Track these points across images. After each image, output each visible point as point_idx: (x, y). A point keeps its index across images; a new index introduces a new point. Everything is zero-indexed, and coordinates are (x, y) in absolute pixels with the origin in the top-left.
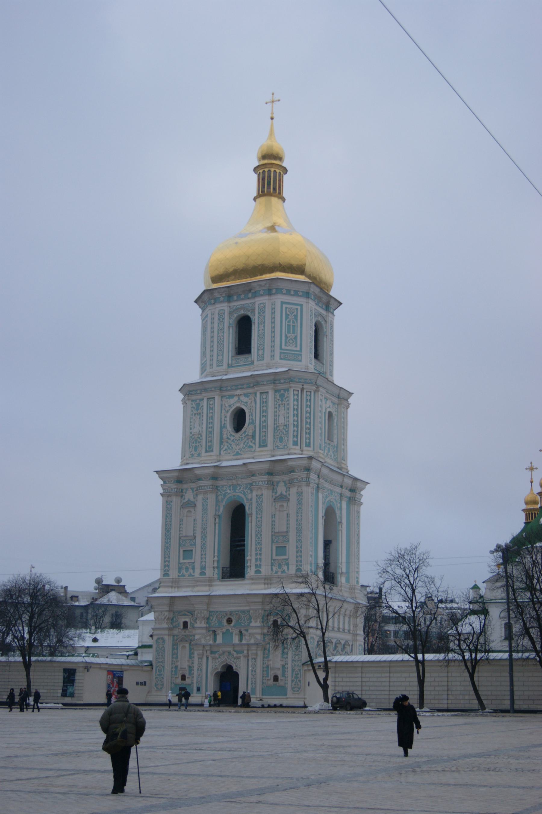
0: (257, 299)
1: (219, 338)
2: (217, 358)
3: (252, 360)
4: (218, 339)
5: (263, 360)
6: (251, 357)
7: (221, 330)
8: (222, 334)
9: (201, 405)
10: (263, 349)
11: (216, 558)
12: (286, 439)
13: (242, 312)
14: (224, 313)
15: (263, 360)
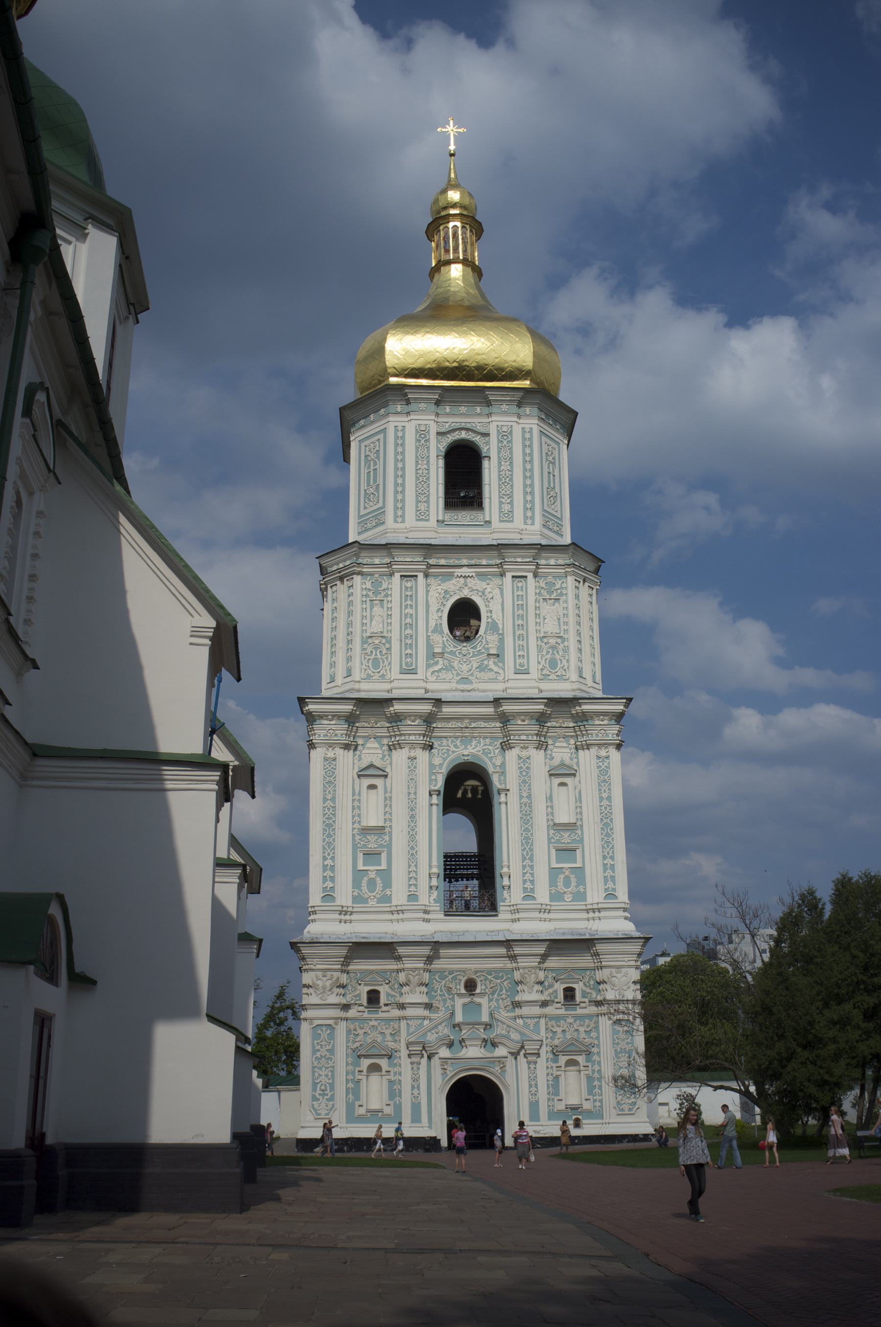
0: (494, 418)
1: (420, 472)
2: (417, 507)
3: (487, 519)
4: (417, 473)
5: (512, 521)
6: (484, 515)
7: (421, 458)
8: (425, 466)
9: (384, 586)
10: (511, 503)
11: (435, 870)
12: (564, 662)
13: (463, 435)
14: (428, 432)
15: (512, 521)
